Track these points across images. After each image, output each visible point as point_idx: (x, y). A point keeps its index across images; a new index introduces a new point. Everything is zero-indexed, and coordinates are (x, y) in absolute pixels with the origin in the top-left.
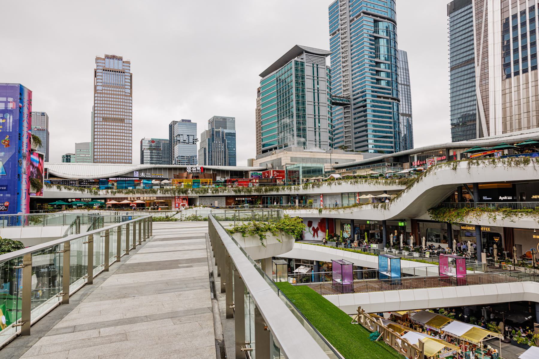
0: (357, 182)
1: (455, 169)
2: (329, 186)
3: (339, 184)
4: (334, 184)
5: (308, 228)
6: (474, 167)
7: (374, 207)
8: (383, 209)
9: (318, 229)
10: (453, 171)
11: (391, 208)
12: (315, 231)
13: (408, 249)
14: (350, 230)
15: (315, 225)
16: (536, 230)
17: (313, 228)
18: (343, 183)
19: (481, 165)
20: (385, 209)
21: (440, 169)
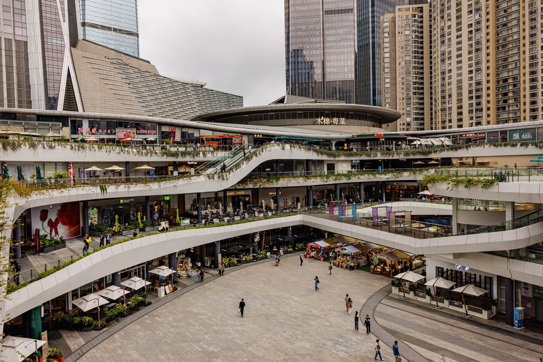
0: (83, 148)
1: (283, 149)
2: (31, 148)
3: (51, 147)
4: (40, 146)
5: (41, 222)
6: (293, 148)
7: (209, 179)
8: (221, 180)
9: (57, 221)
10: (282, 150)
11: (229, 179)
12: (53, 225)
13: (228, 215)
14: (96, 216)
15: (53, 216)
16: (52, 205)
17: (50, 220)
18: (57, 147)
19: (296, 149)
20: (224, 179)
21: (273, 148)
